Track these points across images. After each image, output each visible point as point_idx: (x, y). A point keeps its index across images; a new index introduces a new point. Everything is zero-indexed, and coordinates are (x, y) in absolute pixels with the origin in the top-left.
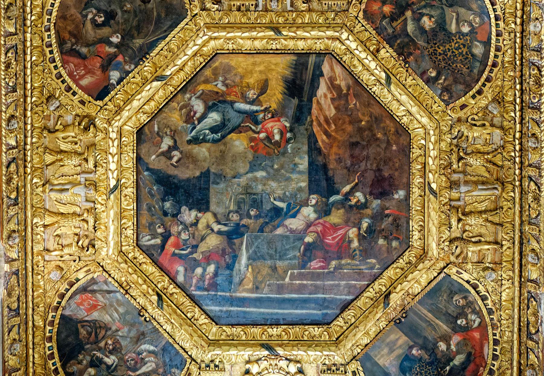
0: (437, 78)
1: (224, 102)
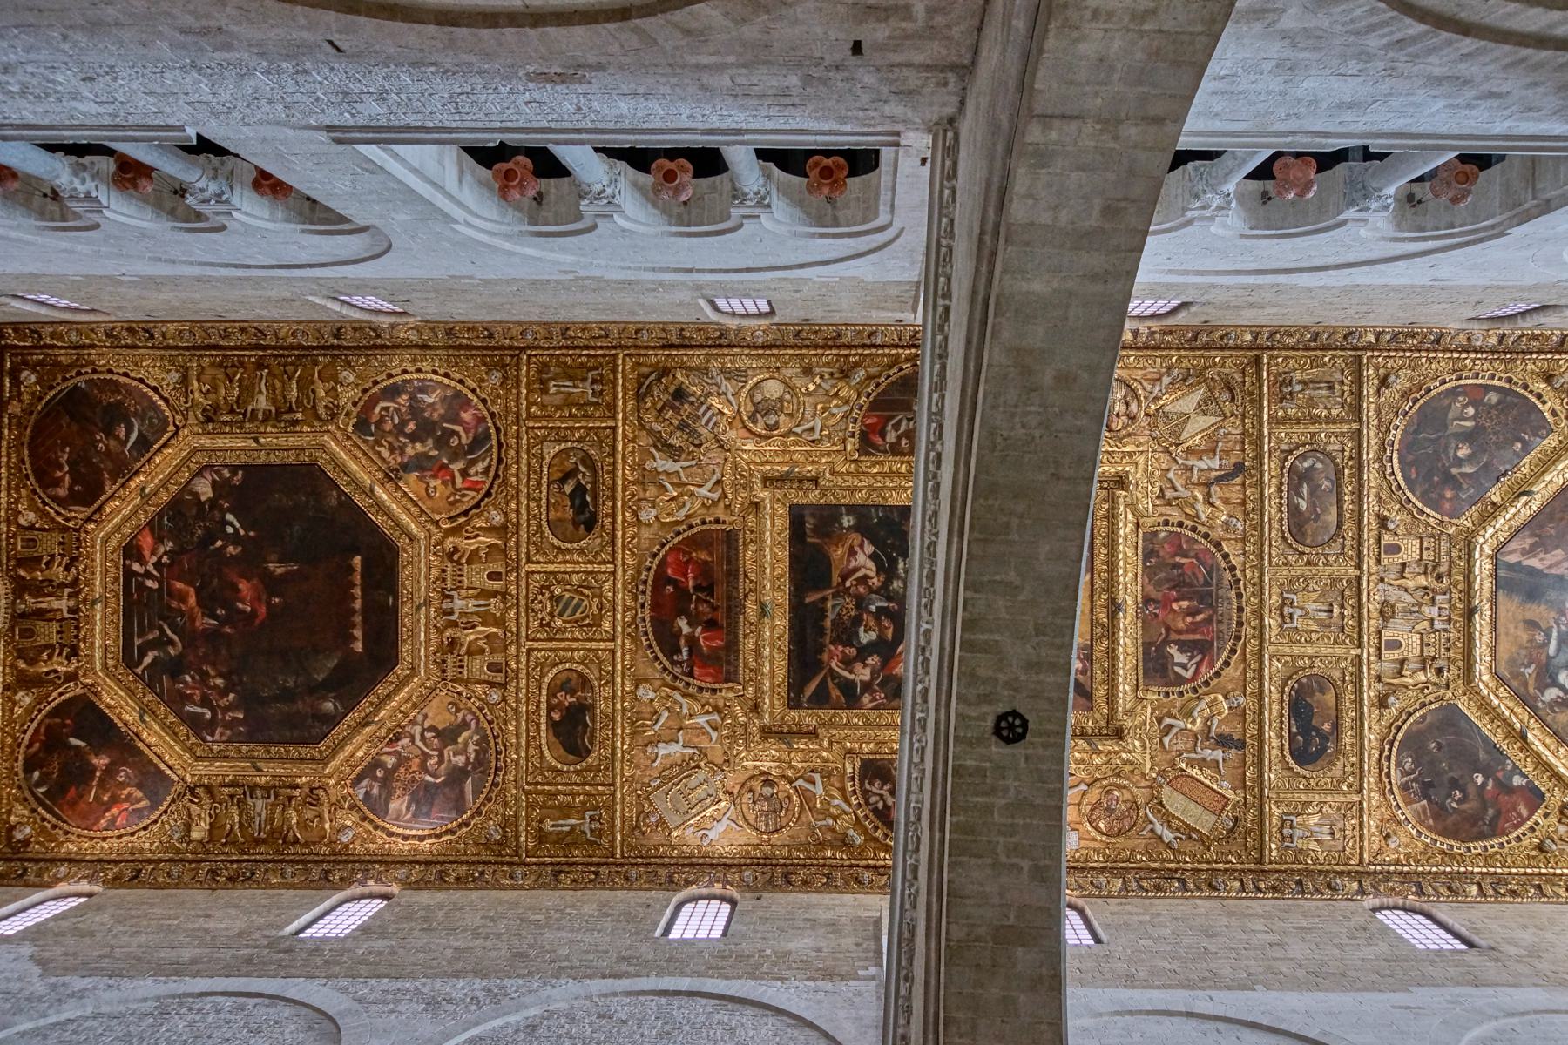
0: (1523, 441)
1: (1547, 665)
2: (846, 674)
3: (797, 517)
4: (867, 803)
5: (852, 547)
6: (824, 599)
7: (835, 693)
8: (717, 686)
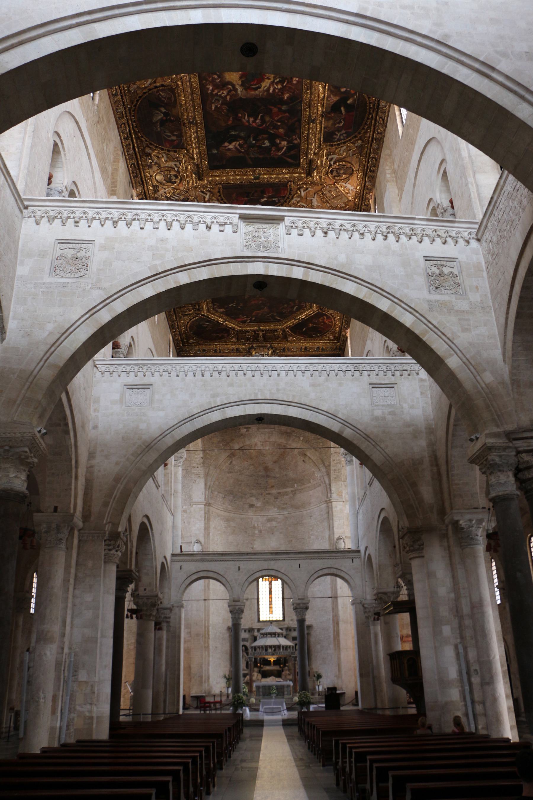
2: (284, 150)
3: (212, 167)
4: (344, 140)
5: (226, 150)
6: (250, 158)
7: (292, 152)
8: (289, 190)
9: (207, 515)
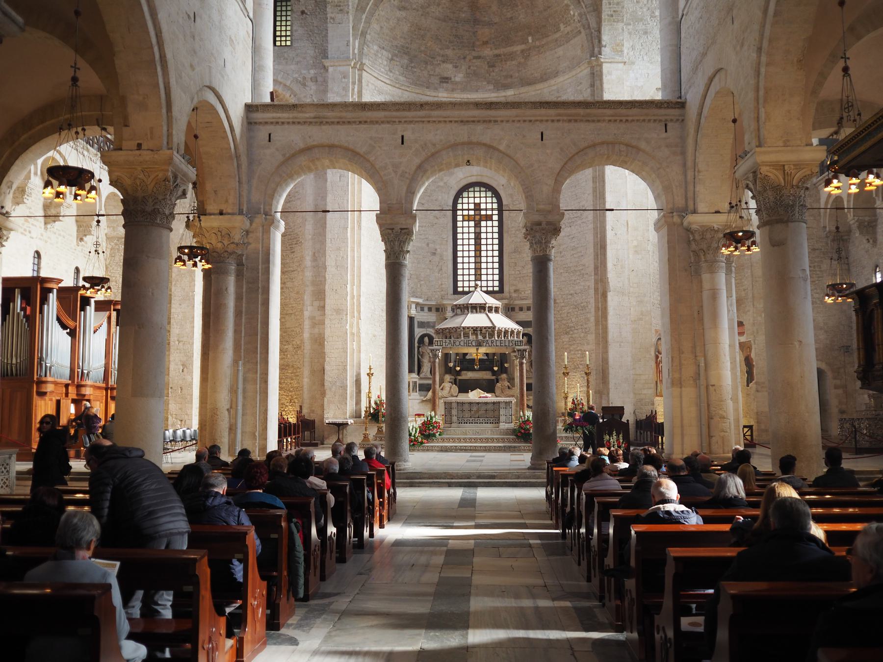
9: (356, 86)
